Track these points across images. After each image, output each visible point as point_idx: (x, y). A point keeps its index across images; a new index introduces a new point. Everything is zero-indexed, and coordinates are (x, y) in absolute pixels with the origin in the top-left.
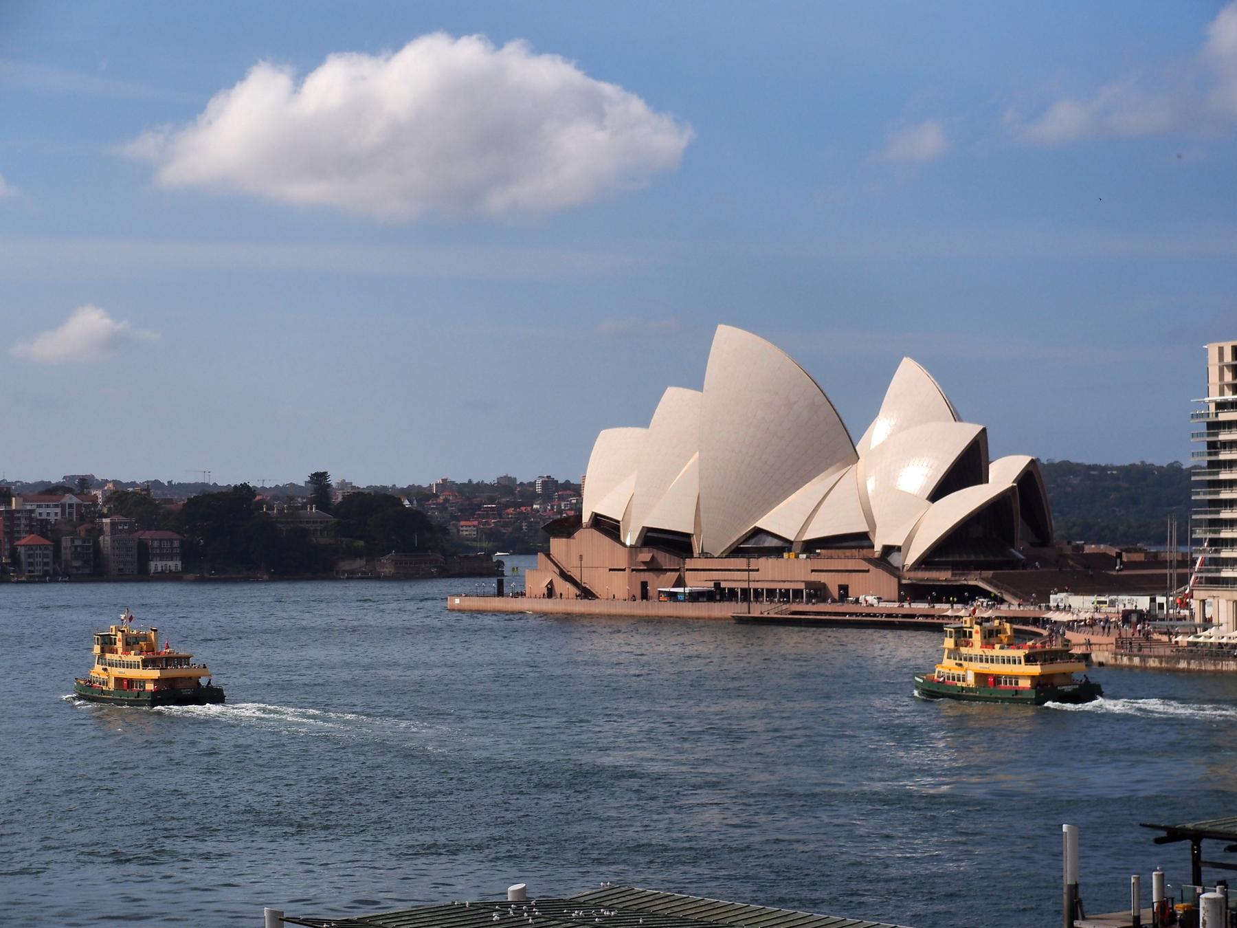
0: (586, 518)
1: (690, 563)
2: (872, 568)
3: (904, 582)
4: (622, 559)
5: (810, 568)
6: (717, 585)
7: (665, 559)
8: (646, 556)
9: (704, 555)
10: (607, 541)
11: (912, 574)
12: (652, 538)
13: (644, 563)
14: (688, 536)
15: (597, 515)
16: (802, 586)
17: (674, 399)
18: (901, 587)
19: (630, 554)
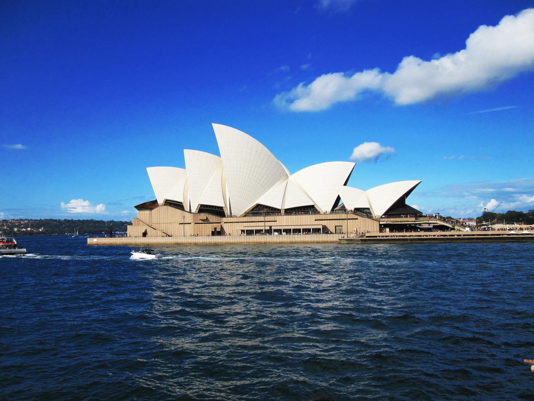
0: (161, 201)
1: (224, 220)
2: (359, 217)
3: (381, 223)
4: (189, 218)
6: (271, 227)
7: (212, 218)
8: (203, 216)
9: (231, 216)
10: (178, 211)
11: (386, 220)
12: (203, 209)
13: (201, 220)
14: (221, 208)
15: (167, 200)
16: (321, 227)
17: (190, 155)
18: (380, 225)
19: (194, 217)
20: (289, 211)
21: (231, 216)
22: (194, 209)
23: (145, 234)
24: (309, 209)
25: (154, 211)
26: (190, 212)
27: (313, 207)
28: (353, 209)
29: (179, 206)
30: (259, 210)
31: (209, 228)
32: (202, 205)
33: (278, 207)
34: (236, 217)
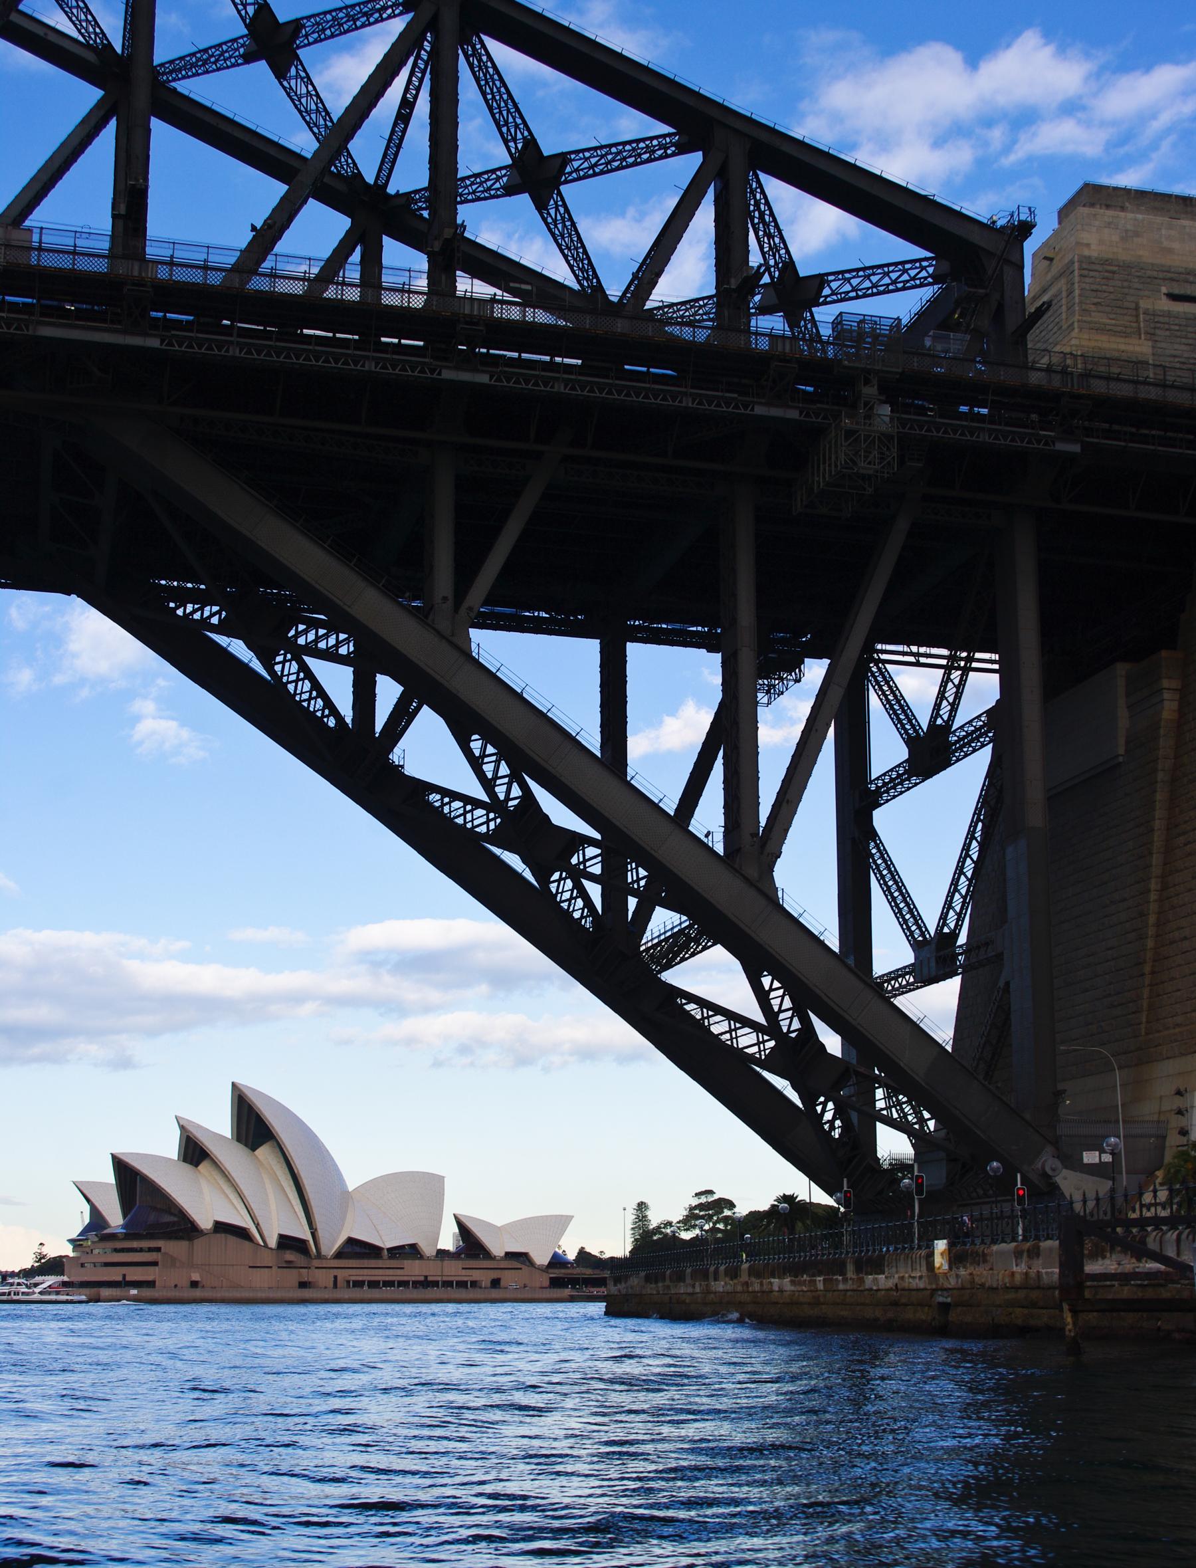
1: (316, 1263)
4: (268, 1259)
5: (460, 1266)
8: (290, 1256)
12: (286, 1242)
14: (303, 1242)
20: (398, 1252)
21: (319, 1255)
22: (273, 1242)
23: (194, 1284)
24: (412, 1251)
25: (199, 1243)
26: (266, 1246)
27: (413, 1246)
28: (502, 1254)
29: (241, 1233)
30: (356, 1249)
31: (292, 1277)
32: (281, 1237)
33: (381, 1245)
34: (325, 1258)
